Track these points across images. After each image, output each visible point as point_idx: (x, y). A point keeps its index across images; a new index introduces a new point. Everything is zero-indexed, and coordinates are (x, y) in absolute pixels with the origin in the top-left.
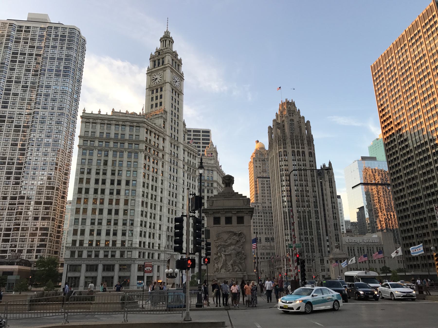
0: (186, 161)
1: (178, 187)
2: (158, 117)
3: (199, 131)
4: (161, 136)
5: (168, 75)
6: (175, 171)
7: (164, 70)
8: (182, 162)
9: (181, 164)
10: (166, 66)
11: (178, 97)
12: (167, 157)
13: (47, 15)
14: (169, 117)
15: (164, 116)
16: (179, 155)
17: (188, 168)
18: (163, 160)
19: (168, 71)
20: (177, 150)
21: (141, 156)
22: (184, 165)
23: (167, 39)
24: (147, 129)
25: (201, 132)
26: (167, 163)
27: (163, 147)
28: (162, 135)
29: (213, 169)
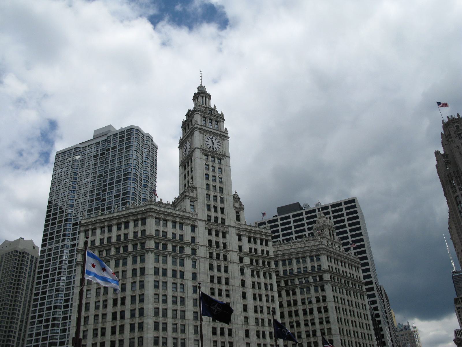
0: (246, 249)
1: (231, 292)
2: (183, 198)
3: (339, 204)
4: (187, 224)
5: (198, 139)
6: (223, 269)
7: (191, 134)
8: (236, 254)
9: (234, 257)
10: (193, 128)
11: (220, 163)
12: (203, 252)
13: (110, 125)
14: (201, 193)
15: (192, 195)
16: (228, 244)
17: (251, 261)
18: (193, 257)
19: (197, 133)
20: (224, 236)
21: (150, 258)
23: (202, 95)
24: (158, 219)
25: (343, 204)
26: (202, 260)
27: (193, 239)
28: (188, 221)
29: (319, 253)
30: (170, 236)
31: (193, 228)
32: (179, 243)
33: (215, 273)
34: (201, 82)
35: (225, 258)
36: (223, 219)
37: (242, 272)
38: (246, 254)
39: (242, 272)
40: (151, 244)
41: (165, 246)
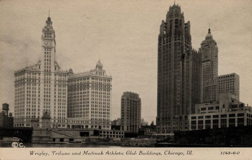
0: (57, 79)
9: (53, 82)
11: (50, 50)
12: (42, 81)
15: (40, 64)
22: (55, 82)
30: (32, 78)
31: (39, 74)
32: (34, 80)
33: (46, 87)
34: (49, 15)
35: (50, 82)
36: (50, 70)
37: (55, 86)
38: (57, 81)
39: (55, 86)
40: (26, 81)
41: (30, 81)
